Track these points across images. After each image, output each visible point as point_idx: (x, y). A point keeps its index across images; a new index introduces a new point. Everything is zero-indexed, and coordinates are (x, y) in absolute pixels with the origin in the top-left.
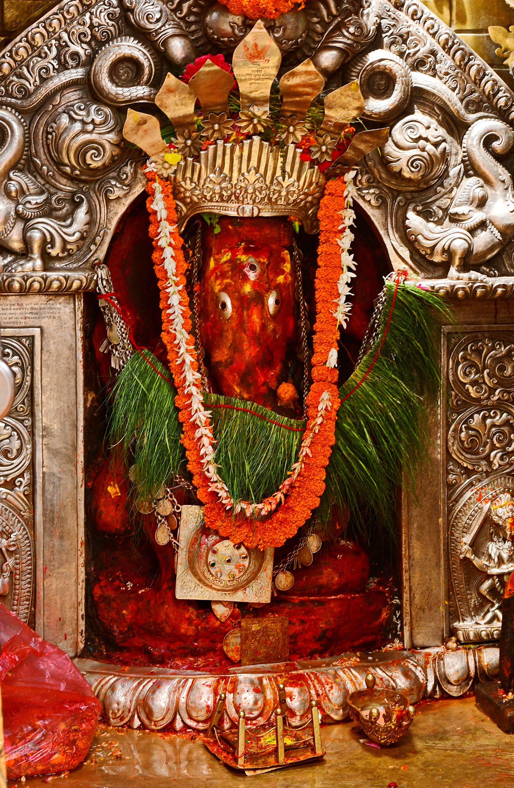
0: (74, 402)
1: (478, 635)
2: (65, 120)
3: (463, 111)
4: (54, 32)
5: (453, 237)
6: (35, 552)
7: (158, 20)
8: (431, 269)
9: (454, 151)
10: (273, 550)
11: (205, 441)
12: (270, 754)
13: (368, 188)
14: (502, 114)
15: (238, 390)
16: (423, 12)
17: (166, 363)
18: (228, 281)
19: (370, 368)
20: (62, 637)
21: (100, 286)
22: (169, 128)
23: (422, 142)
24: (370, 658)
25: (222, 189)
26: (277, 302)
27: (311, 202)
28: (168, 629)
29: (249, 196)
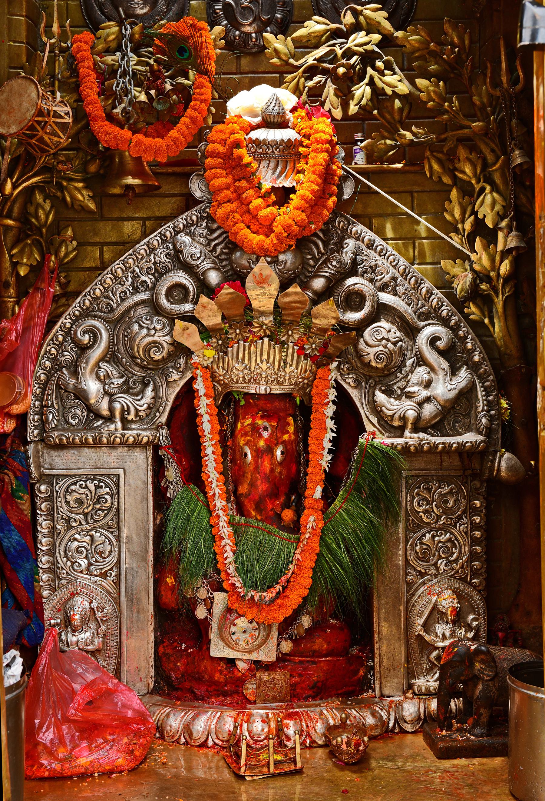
0: (146, 520)
1: (428, 689)
2: (136, 327)
3: (416, 320)
4: (130, 267)
5: (407, 408)
6: (120, 621)
7: (198, 258)
8: (393, 431)
9: (409, 348)
10: (277, 625)
11: (228, 548)
12: (263, 766)
13: (348, 374)
14: (445, 322)
15: (254, 514)
16: (387, 250)
17: (205, 494)
18: (249, 438)
19: (345, 500)
20: (138, 679)
21: (162, 441)
22: (206, 333)
23: (384, 342)
24: (349, 702)
25: (244, 374)
26: (282, 453)
27: (307, 384)
28: (207, 677)
29: (263, 380)
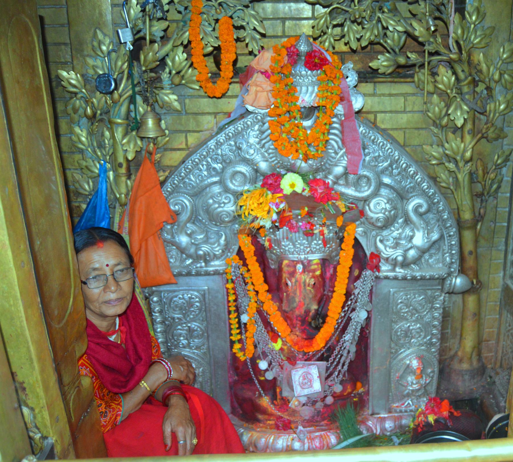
7: (253, 155)
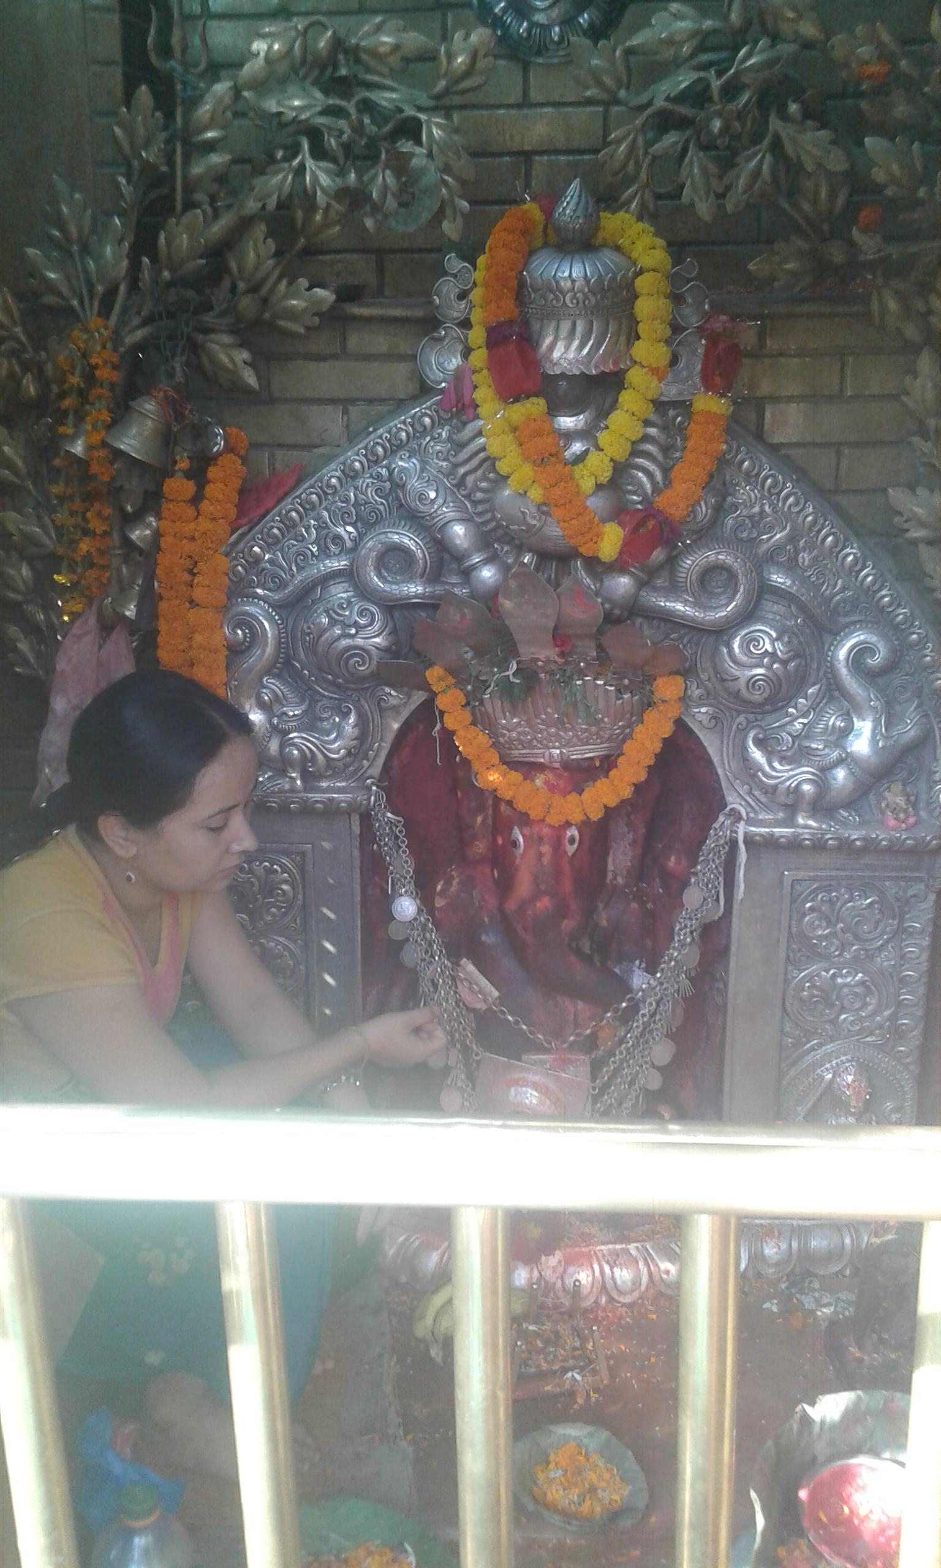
5: (799, 777)
